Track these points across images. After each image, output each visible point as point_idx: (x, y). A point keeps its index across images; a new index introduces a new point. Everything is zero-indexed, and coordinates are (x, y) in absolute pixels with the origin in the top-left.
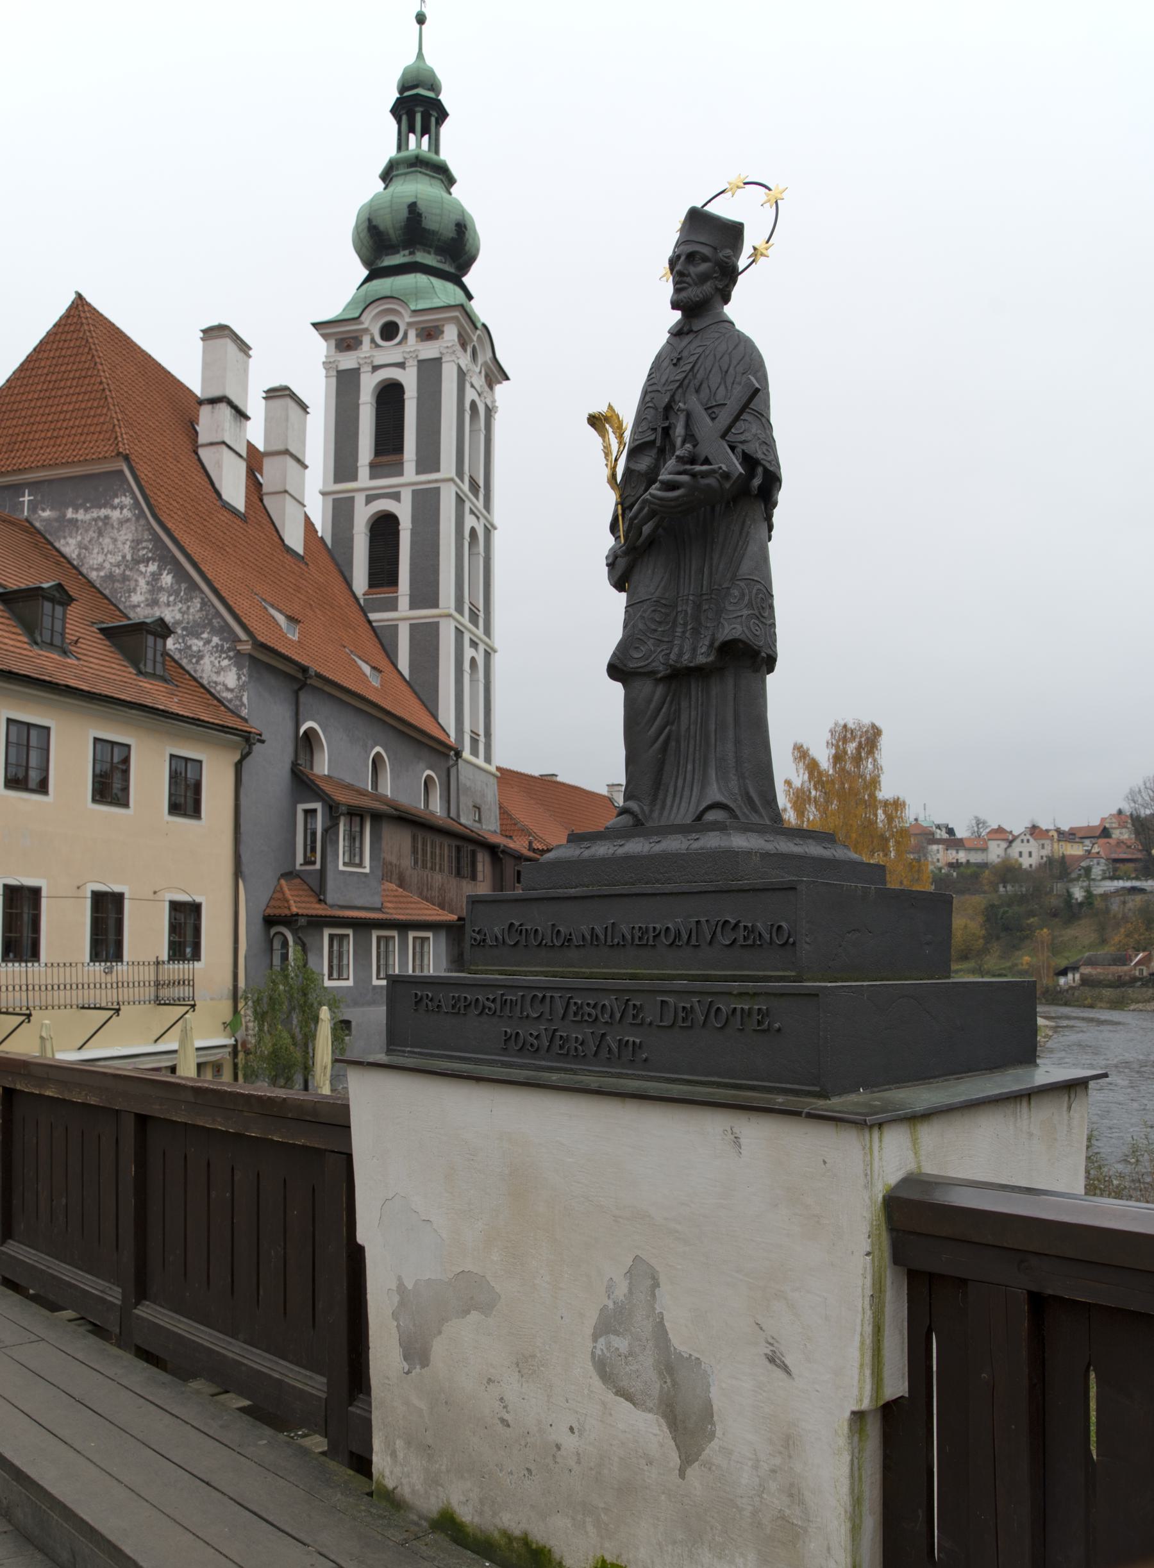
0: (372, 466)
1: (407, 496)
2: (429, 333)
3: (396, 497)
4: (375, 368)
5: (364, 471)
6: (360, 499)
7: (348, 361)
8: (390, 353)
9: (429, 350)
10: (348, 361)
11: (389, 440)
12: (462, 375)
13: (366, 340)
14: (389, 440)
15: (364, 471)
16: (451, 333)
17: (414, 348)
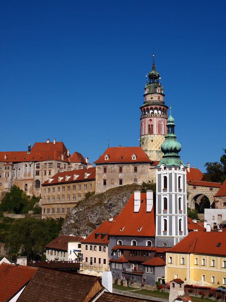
0: (163, 190)
1: (168, 195)
2: (170, 169)
3: (167, 195)
4: (163, 174)
5: (162, 191)
6: (162, 195)
7: (159, 173)
8: (165, 172)
9: (170, 172)
10: (159, 173)
11: (165, 186)
12: (176, 174)
13: (162, 169)
14: (165, 186)
15: (162, 191)
16: (173, 169)
17: (168, 171)
